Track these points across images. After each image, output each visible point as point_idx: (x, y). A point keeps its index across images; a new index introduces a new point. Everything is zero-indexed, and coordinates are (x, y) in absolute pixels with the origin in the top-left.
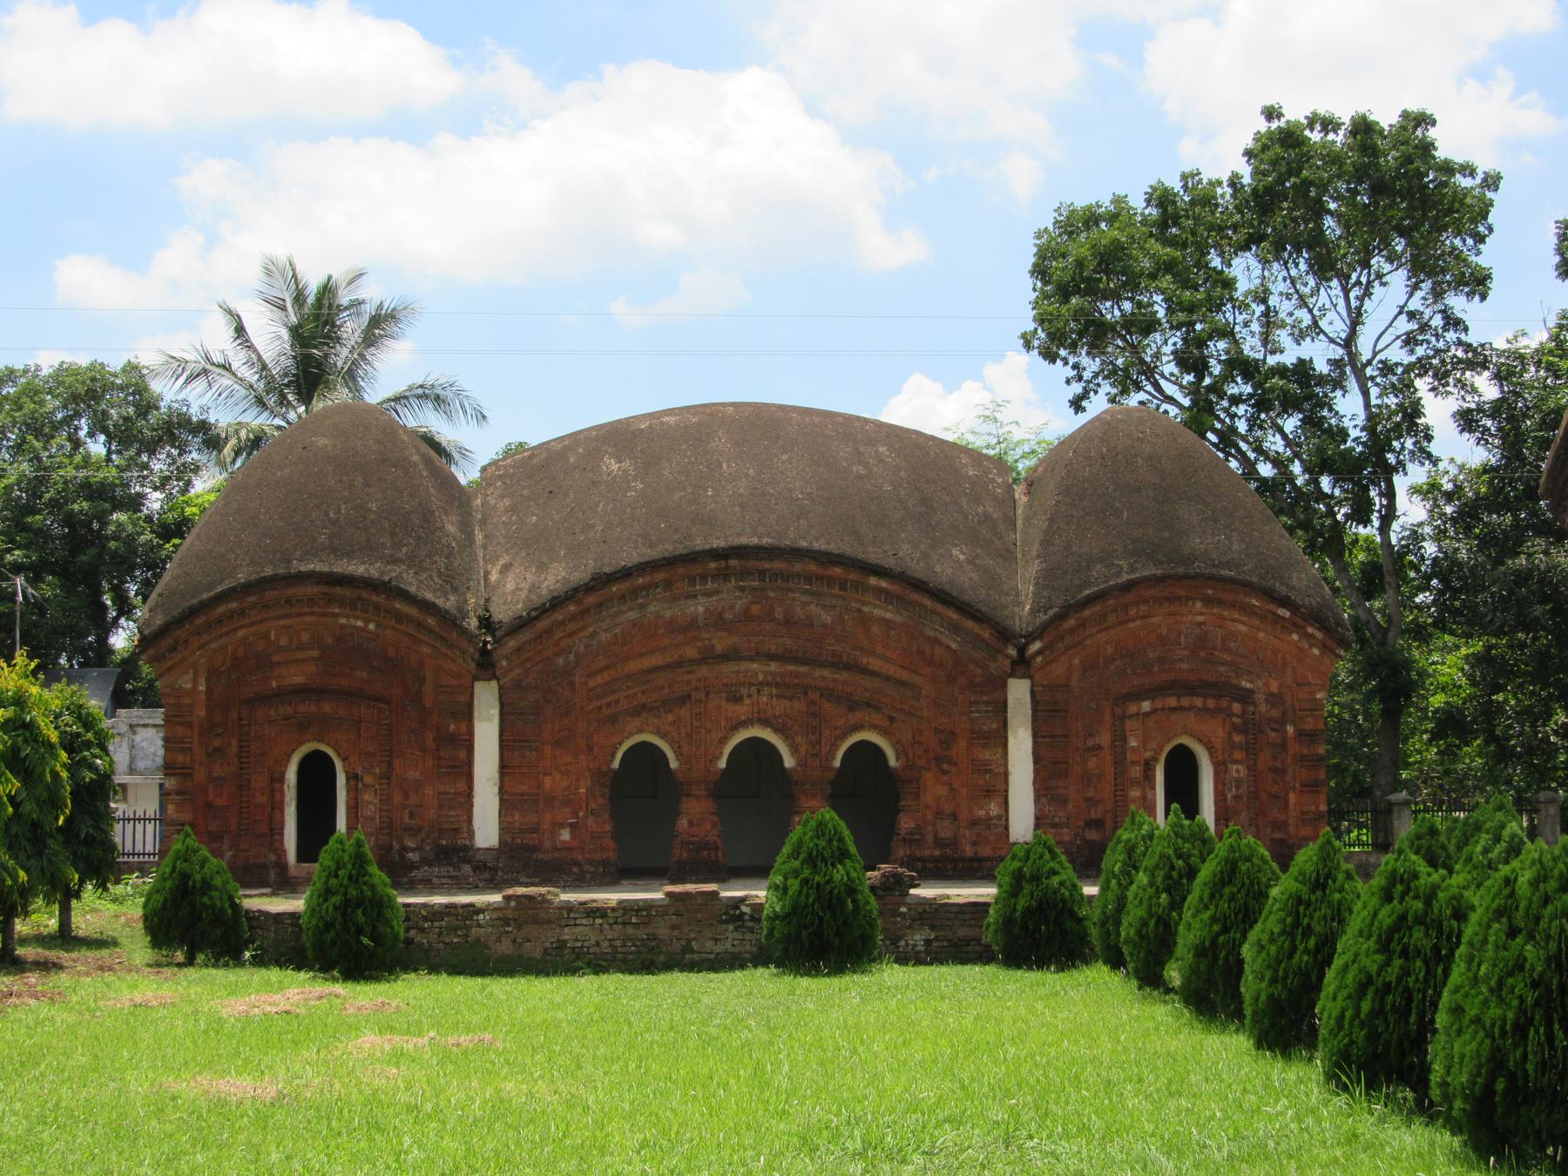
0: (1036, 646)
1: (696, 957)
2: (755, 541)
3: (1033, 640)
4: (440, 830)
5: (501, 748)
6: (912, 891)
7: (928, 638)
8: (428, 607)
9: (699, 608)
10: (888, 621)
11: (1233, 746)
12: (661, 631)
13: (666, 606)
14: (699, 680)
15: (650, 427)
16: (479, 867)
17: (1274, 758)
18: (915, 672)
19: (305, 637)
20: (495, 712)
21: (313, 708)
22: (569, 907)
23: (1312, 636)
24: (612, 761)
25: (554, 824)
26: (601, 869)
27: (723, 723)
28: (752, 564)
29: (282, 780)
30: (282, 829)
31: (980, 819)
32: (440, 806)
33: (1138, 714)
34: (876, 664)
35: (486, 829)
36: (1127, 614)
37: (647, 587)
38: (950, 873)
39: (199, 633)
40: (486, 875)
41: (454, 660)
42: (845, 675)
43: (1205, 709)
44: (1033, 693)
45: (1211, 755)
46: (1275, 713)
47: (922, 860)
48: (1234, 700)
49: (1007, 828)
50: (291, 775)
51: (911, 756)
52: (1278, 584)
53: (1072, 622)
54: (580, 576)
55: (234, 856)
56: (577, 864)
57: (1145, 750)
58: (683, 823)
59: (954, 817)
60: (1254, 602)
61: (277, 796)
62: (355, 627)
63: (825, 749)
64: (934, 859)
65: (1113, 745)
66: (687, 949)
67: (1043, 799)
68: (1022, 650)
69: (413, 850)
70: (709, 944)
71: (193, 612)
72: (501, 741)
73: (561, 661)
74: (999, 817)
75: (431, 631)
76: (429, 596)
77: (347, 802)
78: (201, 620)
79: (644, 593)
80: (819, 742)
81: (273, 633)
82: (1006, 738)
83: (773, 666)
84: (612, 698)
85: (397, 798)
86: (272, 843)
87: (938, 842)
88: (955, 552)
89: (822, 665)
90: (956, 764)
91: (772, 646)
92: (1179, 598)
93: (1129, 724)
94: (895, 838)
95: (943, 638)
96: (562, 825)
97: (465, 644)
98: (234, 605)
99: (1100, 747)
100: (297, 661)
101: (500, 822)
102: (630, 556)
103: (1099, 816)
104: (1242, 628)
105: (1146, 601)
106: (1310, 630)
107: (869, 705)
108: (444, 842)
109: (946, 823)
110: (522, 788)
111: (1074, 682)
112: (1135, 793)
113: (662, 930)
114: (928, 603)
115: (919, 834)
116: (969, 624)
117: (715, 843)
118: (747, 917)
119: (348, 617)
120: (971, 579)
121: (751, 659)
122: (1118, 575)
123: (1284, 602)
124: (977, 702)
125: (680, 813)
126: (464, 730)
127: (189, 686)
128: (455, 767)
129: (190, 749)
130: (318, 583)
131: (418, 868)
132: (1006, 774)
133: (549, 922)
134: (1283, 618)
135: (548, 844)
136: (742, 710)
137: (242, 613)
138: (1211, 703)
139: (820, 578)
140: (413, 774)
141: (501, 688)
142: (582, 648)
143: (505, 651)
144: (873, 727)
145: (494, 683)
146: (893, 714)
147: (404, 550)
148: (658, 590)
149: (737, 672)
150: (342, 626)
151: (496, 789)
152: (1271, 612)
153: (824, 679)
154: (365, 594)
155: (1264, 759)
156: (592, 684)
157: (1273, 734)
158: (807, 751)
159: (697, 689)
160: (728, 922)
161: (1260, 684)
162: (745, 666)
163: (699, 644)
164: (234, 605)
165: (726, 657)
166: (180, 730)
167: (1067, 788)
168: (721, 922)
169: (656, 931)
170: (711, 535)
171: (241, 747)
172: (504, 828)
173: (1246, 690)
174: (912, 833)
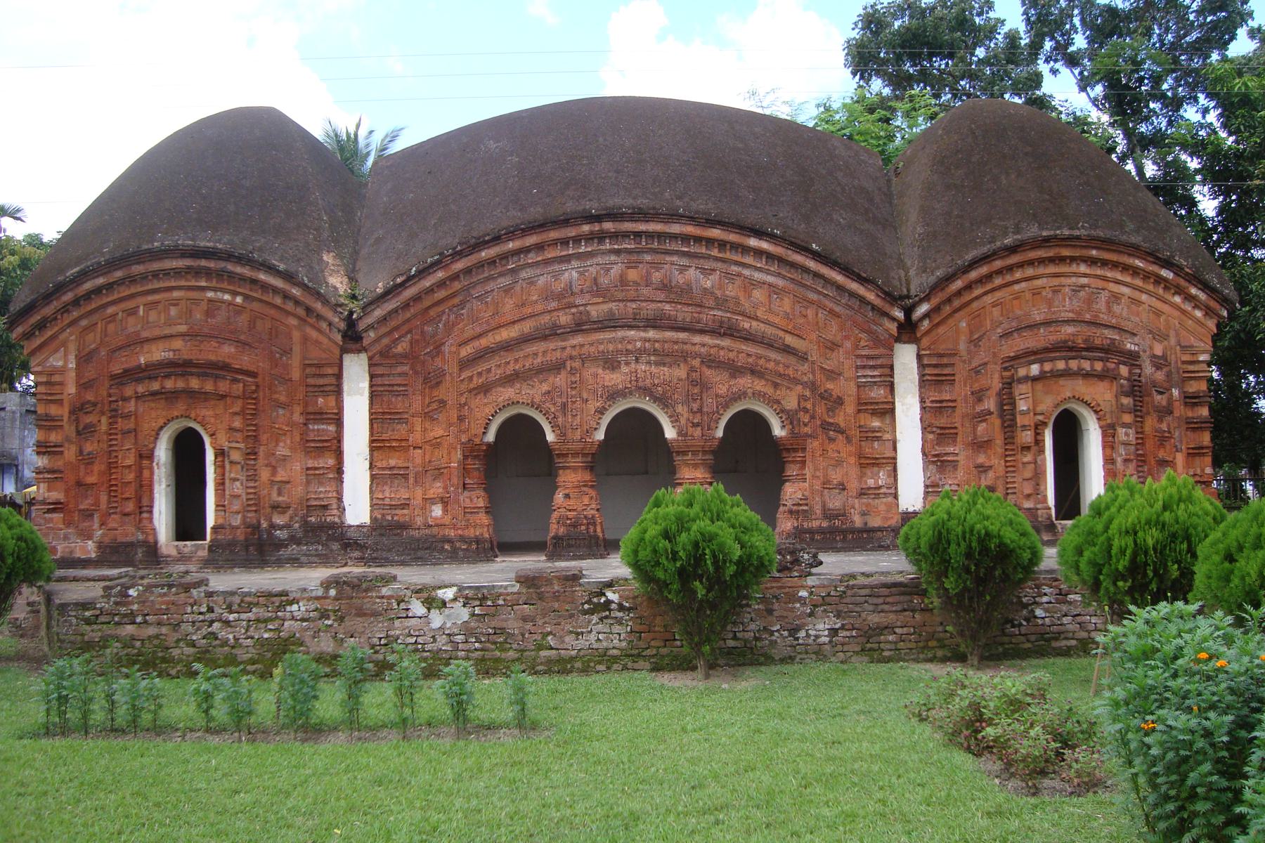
0: (924, 308)
3: (921, 301)
4: (308, 506)
5: (371, 421)
7: (812, 302)
8: (288, 277)
9: (571, 274)
10: (770, 285)
11: (1122, 409)
12: (534, 298)
13: (538, 271)
16: (355, 545)
20: (365, 385)
24: (484, 433)
25: (425, 500)
29: (151, 456)
32: (308, 482)
38: (839, 545)
39: (68, 311)
40: (357, 554)
42: (726, 342)
44: (919, 357)
45: (1099, 419)
46: (1160, 376)
47: (811, 532)
49: (896, 496)
50: (163, 453)
53: (958, 284)
55: (103, 535)
56: (450, 541)
57: (1035, 414)
58: (559, 497)
59: (842, 487)
60: (1139, 263)
61: (146, 473)
62: (223, 302)
64: (821, 531)
68: (908, 311)
69: (281, 528)
70: (569, 639)
72: (371, 414)
75: (297, 302)
76: (293, 268)
77: (215, 479)
78: (68, 297)
79: (515, 258)
80: (700, 410)
81: (141, 308)
82: (893, 403)
83: (651, 334)
84: (485, 366)
86: (140, 521)
87: (828, 514)
89: (702, 332)
90: (842, 432)
91: (649, 309)
94: (782, 509)
96: (433, 501)
97: (329, 314)
98: (101, 281)
99: (991, 413)
101: (372, 499)
105: (1031, 263)
106: (1193, 291)
108: (313, 519)
110: (392, 462)
111: (962, 346)
115: (807, 505)
116: (854, 286)
117: (593, 516)
118: (613, 606)
119: (215, 290)
121: (631, 327)
122: (1005, 235)
123: (1167, 264)
124: (864, 367)
125: (557, 487)
126: (333, 403)
127: (60, 363)
131: (286, 546)
133: (375, 614)
134: (1165, 280)
135: (419, 521)
136: (615, 379)
138: (1099, 366)
139: (698, 240)
141: (370, 359)
142: (452, 317)
143: (369, 320)
144: (758, 395)
148: (530, 255)
150: (210, 300)
153: (704, 345)
155: (1150, 423)
156: (466, 351)
157: (1158, 397)
159: (571, 358)
160: (590, 612)
162: (620, 333)
163: (574, 310)
168: (585, 612)
169: (504, 625)
170: (585, 197)
171: (110, 424)
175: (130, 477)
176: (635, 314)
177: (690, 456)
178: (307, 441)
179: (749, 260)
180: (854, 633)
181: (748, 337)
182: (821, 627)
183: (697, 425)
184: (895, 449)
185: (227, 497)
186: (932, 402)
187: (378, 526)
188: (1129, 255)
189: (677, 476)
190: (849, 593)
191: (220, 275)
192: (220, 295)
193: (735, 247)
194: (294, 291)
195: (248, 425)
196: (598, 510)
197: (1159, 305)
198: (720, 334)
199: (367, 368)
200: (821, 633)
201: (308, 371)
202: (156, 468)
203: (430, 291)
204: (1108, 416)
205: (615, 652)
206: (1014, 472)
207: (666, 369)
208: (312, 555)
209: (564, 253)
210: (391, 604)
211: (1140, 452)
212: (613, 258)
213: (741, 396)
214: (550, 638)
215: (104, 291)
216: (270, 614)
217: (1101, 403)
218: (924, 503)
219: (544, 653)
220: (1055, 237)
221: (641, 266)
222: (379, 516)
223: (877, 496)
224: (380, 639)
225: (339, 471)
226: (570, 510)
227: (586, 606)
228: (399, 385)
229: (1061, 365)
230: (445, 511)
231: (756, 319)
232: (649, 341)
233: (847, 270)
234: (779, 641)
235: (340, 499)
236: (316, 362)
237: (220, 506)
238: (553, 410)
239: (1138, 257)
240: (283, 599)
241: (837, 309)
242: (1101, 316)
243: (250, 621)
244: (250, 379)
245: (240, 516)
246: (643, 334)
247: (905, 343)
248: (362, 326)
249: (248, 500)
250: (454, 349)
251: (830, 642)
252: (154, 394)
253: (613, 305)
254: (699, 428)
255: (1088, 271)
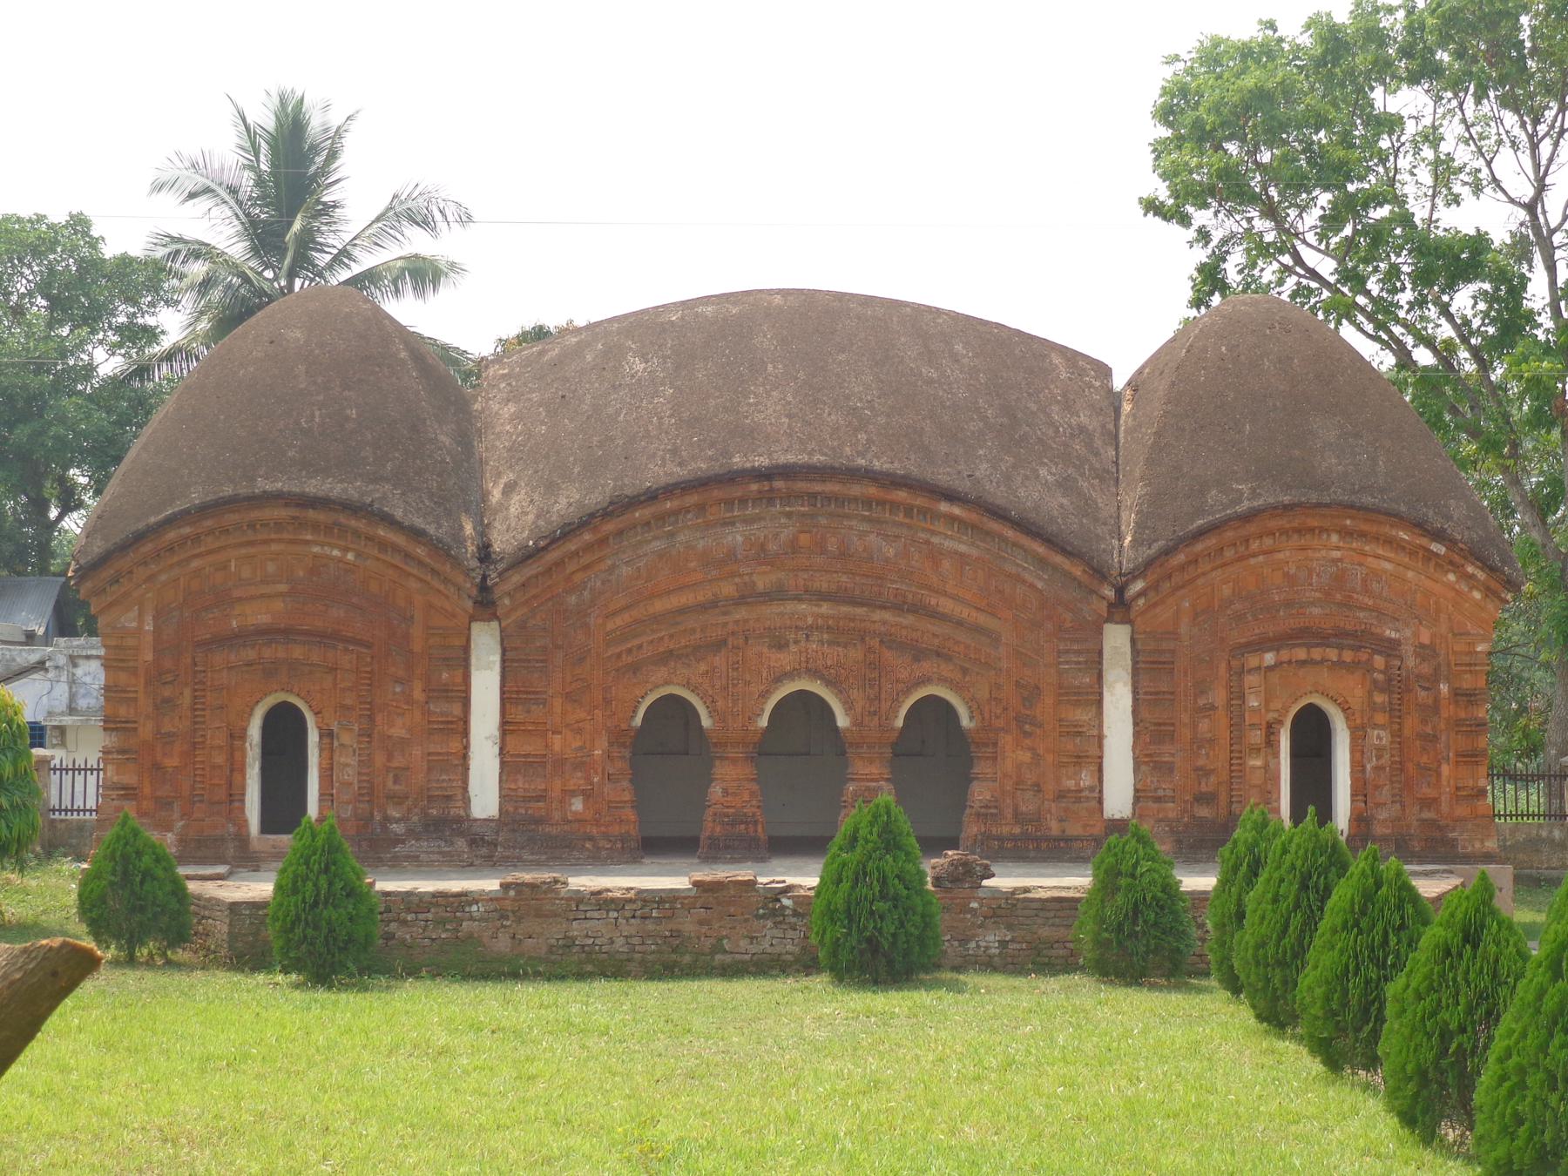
0: (1139, 586)
1: (728, 959)
2: (803, 458)
3: (1135, 578)
4: (429, 797)
5: (502, 700)
6: (985, 883)
7: (1010, 576)
8: (417, 534)
9: (736, 537)
10: (962, 555)
11: (1373, 707)
12: (692, 565)
13: (698, 535)
14: (737, 622)
15: (682, 318)
17: (1424, 722)
18: (993, 615)
19: (271, 567)
21: (281, 654)
22: (579, 898)
23: (1472, 577)
26: (619, 845)
27: (764, 675)
28: (801, 486)
29: (243, 736)
30: (243, 794)
31: (1069, 791)
32: (430, 770)
33: (1259, 668)
34: (946, 605)
35: (484, 797)
36: (1247, 548)
37: (675, 513)
38: (1032, 854)
39: (145, 563)
40: (484, 851)
41: (447, 597)
42: (909, 620)
43: (1340, 664)
44: (1133, 641)
45: (1347, 718)
46: (1426, 669)
47: (1000, 839)
48: (1375, 652)
49: (1100, 801)
51: (987, 715)
52: (1431, 513)
53: (1181, 558)
54: (596, 499)
56: (591, 839)
57: (1268, 711)
58: (716, 791)
60: (1403, 535)
61: (237, 754)
62: (332, 558)
63: (885, 706)
64: (1014, 838)
65: (1229, 705)
66: (718, 948)
67: (1144, 768)
68: (1120, 591)
69: (398, 821)
70: (744, 943)
71: (139, 538)
72: (503, 693)
73: (573, 599)
74: (1091, 789)
75: (420, 563)
76: (419, 522)
77: (320, 764)
78: (148, 547)
79: (672, 519)
81: (233, 564)
82: (1101, 694)
83: (825, 608)
84: (636, 642)
85: (380, 759)
86: (230, 812)
87: (1018, 817)
88: (1043, 472)
90: (1041, 726)
91: (823, 583)
92: (1312, 530)
93: (1251, 680)
94: (968, 811)
95: (1027, 576)
96: (573, 793)
97: (460, 579)
98: (187, 530)
99: (1213, 708)
100: (262, 596)
102: (657, 472)
103: (1211, 789)
104: (1388, 566)
106: (1470, 569)
107: (938, 654)
109: (1028, 795)
110: (528, 749)
111: (1183, 629)
112: (1257, 762)
113: (688, 925)
114: (1009, 533)
115: (996, 807)
116: (1059, 559)
117: (754, 815)
119: (322, 546)
120: (1061, 506)
121: (798, 599)
122: (1239, 501)
123: (1438, 536)
124: (1067, 652)
125: (712, 780)
126: (459, 680)
127: (134, 624)
128: (448, 722)
129: (135, 700)
130: (286, 505)
131: (403, 842)
132: (1100, 738)
134: (1437, 555)
135: (557, 815)
136: (785, 660)
137: (196, 539)
138: (1348, 656)
139: (881, 503)
140: (398, 731)
142: (599, 584)
143: (508, 587)
144: (942, 680)
145: (495, 624)
146: (967, 665)
147: (389, 466)
148: (689, 516)
149: (782, 614)
150: (315, 556)
151: (496, 750)
152: (1421, 547)
153: (884, 623)
154: (342, 519)
155: (1411, 724)
156: (610, 626)
157: (1424, 693)
158: (863, 708)
160: (763, 917)
161: (1408, 633)
162: (790, 607)
163: (737, 580)
164: (187, 530)
165: (769, 596)
166: (123, 678)
167: (1173, 755)
171: (195, 697)
172: (504, 797)
173: (1390, 640)
174: (986, 807)
175: (219, 759)
176: (805, 584)
177: (865, 749)
178: (429, 722)
179: (939, 526)
180: (1024, 946)
181: (934, 615)
182: (991, 939)
183: (875, 713)
184: (1101, 746)
185: (336, 785)
186: (1146, 693)
187: (506, 819)
188: (1392, 526)
189: (850, 770)
190: (1020, 905)
191: (328, 529)
192: (327, 550)
193: (924, 512)
194: (419, 551)
195: (361, 703)
196: (759, 807)
197: (1429, 584)
198: (903, 610)
200: (991, 944)
202: (249, 748)
203: (576, 554)
204: (1357, 715)
205: (789, 957)
206: (1240, 777)
207: (840, 649)
208: (433, 853)
209: (728, 515)
210: (570, 905)
211: (1397, 759)
212: (782, 521)
213: (924, 681)
214: (725, 941)
215: (189, 543)
216: (448, 914)
217: (1350, 700)
218: (1134, 809)
219: (718, 957)
220: (1300, 505)
221: (815, 530)
222: (511, 809)
223: (1078, 800)
224: (558, 940)
225: (465, 756)
226: (728, 807)
227: (761, 911)
228: (537, 661)
229: (1301, 654)
231: (945, 594)
232: (822, 616)
233: (1049, 541)
234: (949, 951)
235: (465, 789)
237: (326, 796)
238: (710, 692)
239: (1403, 530)
240: (463, 900)
241: (1040, 585)
242: (1355, 596)
243: (427, 921)
244: (365, 651)
245: (350, 807)
246: (815, 609)
247: (1117, 623)
248: (497, 592)
249: (359, 788)
250: (600, 621)
251: (1000, 953)
252: (249, 664)
253: (781, 575)
254: (876, 718)
255: (1341, 544)
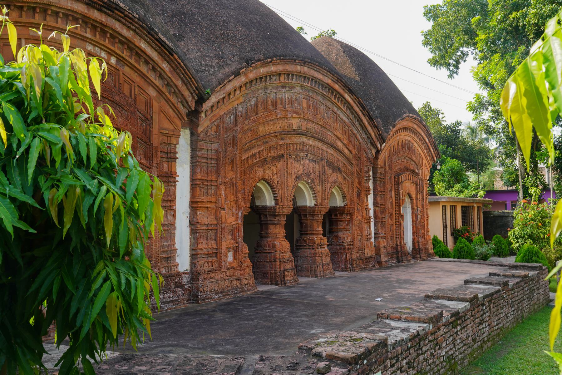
104: (416, 145)
115: (352, 245)
116: (369, 128)
199: (189, 142)
201: (165, 139)
208: (168, 302)
230: (235, 258)
236: (167, 132)
